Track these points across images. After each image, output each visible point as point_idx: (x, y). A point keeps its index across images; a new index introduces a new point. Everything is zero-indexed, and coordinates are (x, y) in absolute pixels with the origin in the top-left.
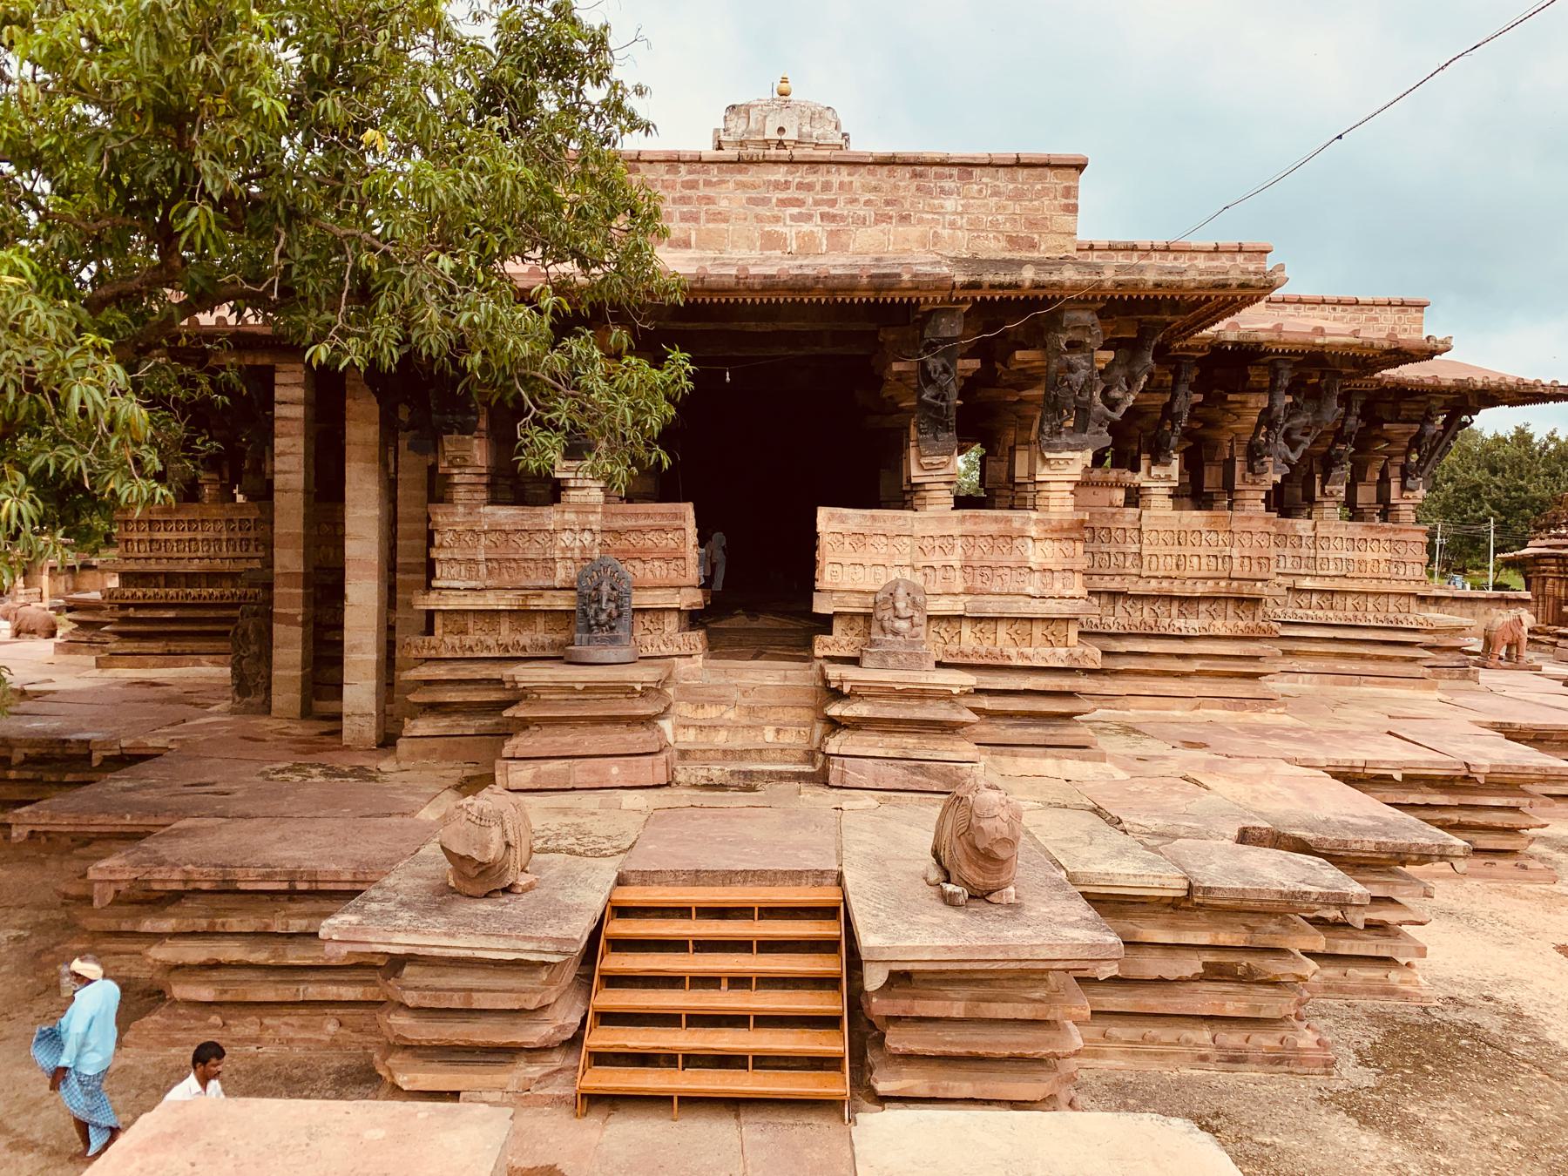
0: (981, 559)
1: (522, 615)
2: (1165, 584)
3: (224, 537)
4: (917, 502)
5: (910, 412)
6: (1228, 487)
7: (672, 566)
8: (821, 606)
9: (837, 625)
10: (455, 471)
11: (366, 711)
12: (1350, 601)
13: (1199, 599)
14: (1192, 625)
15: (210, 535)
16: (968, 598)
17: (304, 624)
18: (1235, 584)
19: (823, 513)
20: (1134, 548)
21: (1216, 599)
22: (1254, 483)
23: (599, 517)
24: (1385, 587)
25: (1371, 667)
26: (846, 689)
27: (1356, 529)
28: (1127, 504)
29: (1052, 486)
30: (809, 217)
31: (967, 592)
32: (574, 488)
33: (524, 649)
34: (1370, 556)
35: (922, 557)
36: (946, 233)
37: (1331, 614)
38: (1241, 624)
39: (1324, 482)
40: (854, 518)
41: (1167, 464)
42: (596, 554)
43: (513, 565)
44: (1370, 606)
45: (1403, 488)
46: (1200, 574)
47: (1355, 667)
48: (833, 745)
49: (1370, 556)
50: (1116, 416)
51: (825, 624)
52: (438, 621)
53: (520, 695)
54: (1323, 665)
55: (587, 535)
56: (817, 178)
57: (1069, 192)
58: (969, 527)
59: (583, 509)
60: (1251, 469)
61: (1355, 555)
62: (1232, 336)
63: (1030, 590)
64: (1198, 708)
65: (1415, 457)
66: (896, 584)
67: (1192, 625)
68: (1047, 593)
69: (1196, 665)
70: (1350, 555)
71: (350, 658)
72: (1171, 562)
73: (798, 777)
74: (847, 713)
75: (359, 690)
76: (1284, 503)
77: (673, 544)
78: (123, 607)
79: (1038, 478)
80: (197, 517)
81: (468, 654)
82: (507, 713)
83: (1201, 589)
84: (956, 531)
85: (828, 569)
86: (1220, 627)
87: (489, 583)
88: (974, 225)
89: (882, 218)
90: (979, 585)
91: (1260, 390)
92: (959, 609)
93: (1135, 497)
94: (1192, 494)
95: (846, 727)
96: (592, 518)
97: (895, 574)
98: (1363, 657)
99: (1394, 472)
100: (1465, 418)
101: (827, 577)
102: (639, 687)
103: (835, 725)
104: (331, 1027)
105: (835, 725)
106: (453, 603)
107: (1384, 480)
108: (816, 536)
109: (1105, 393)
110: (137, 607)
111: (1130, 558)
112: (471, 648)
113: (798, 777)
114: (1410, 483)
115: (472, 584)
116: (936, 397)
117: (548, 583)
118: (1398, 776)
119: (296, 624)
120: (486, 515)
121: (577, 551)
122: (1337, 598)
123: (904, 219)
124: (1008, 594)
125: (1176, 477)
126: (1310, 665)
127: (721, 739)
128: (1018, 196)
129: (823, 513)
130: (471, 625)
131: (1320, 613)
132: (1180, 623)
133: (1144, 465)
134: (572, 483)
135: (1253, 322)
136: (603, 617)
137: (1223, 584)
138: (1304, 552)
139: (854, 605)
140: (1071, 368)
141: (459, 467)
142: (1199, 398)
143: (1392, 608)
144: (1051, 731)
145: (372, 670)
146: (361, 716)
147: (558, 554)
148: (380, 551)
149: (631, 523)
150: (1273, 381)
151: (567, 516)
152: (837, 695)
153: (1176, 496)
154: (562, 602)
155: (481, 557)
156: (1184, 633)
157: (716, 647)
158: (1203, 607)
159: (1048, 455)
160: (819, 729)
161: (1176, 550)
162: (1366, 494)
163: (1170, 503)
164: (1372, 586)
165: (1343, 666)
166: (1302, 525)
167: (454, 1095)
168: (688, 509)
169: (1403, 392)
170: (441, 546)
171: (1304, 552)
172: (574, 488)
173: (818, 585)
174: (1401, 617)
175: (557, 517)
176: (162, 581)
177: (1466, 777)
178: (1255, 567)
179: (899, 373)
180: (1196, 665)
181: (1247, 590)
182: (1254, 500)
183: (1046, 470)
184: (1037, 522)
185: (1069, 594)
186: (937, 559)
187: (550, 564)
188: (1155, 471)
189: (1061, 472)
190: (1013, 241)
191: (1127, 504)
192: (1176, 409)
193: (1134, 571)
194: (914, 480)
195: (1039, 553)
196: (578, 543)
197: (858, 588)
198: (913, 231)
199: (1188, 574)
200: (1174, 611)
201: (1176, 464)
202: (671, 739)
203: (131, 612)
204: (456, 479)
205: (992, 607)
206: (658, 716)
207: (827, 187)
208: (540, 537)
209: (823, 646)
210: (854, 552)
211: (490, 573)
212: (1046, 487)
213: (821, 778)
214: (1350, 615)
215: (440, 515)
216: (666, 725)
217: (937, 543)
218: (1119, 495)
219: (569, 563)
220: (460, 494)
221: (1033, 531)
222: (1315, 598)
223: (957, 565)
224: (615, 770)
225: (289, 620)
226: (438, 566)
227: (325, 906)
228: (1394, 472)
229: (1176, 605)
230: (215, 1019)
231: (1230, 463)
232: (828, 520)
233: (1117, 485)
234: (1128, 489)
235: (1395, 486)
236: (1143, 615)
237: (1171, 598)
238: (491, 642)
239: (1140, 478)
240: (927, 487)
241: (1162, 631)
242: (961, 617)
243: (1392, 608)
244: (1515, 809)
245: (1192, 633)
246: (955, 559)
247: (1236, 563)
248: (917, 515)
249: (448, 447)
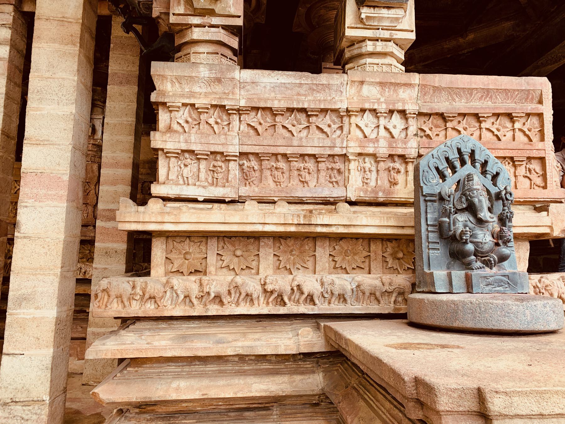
1: (298, 242)
7: (521, 171)
10: (196, 20)
11: (34, 395)
23: (414, 92)
32: (372, 54)
33: (311, 299)
43: (282, 164)
52: (158, 251)
55: (396, 119)
81: (214, 310)
87: (244, 191)
106: (189, 219)
112: (218, 299)
117: (337, 192)
120: (242, 85)
121: (383, 143)
130: (212, 259)
134: (369, 47)
136: (485, 238)
145: (47, 333)
146: (25, 403)
148: (74, 166)
149: (461, 105)
151: (366, 90)
154: (370, 222)
170: (169, 129)
172: (372, 54)
175: (351, 91)
187: (339, 165)
196: (382, 132)
204: (196, 34)
208: (324, 121)
211: (246, 178)
215: (168, 78)
219: (369, 163)
226: (162, 164)
238: (252, 285)
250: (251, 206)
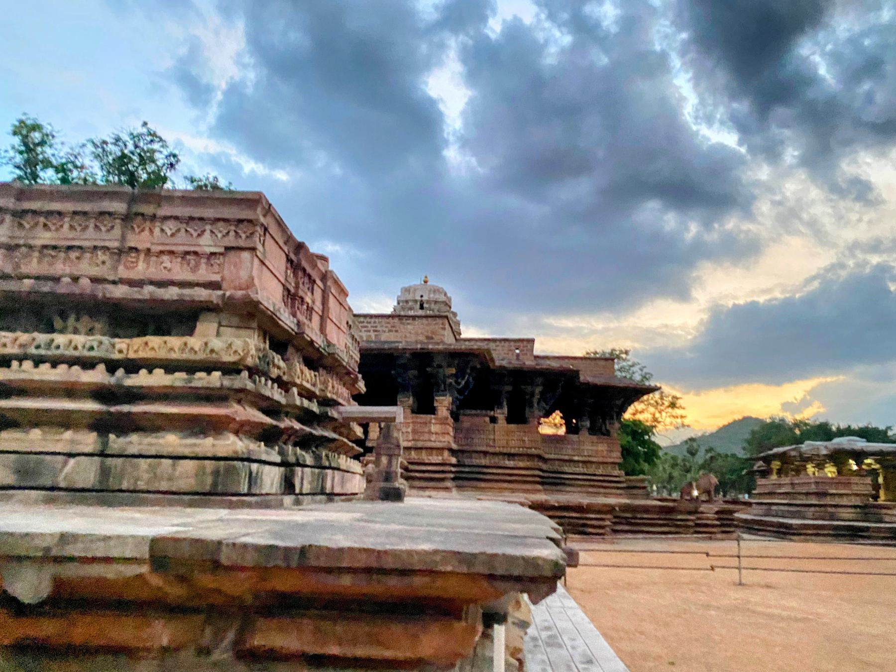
14: (511, 463)
20: (492, 437)
24: (605, 460)
30: (369, 331)
31: (413, 440)
36: (408, 335)
50: (460, 387)
56: (373, 320)
61: (594, 448)
67: (511, 463)
86: (521, 464)
88: (417, 334)
89: (390, 331)
92: (410, 444)
93: (494, 420)
123: (396, 331)
128: (428, 325)
132: (507, 462)
153: (509, 420)
161: (506, 438)
164: (601, 460)
165: (590, 490)
189: (444, 403)
190: (427, 337)
198: (399, 335)
205: (420, 444)
207: (375, 322)
218: (487, 419)
233: (487, 415)
236: (496, 460)
237: (505, 454)
246: (410, 430)
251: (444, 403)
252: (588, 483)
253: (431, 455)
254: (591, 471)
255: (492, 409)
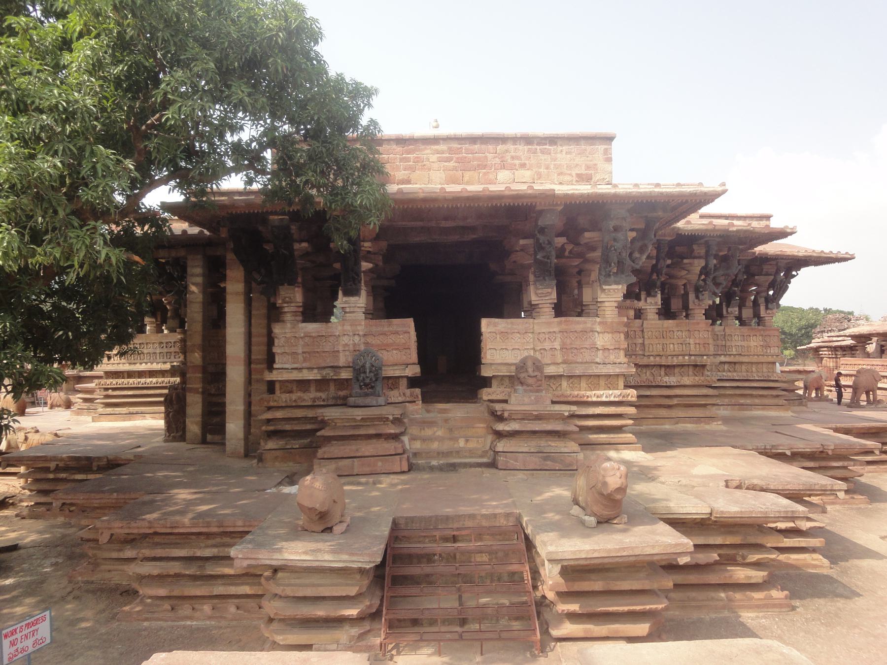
0: (571, 344)
1: (322, 384)
2: (658, 359)
3: (158, 351)
4: (534, 314)
5: (529, 266)
6: (686, 307)
7: (403, 353)
8: (486, 372)
9: (494, 383)
12: (744, 367)
13: (674, 366)
14: (671, 380)
15: (151, 351)
16: (564, 366)
17: (203, 393)
18: (693, 357)
19: (484, 322)
20: (640, 341)
21: (683, 366)
22: (699, 305)
24: (762, 359)
25: (757, 401)
26: (506, 415)
27: (745, 329)
28: (636, 318)
29: (607, 304)
31: (564, 362)
34: (752, 344)
35: (539, 344)
37: (735, 374)
38: (696, 378)
39: (728, 306)
40: (501, 324)
41: (655, 296)
42: (362, 348)
44: (754, 369)
45: (767, 308)
46: (674, 353)
47: (748, 401)
48: (501, 446)
49: (752, 344)
51: (486, 382)
52: (277, 386)
53: (323, 424)
54: (733, 401)
57: (606, 152)
58: (564, 327)
59: (354, 324)
60: (697, 297)
61: (743, 343)
62: (689, 227)
63: (598, 360)
64: (677, 423)
65: (771, 293)
66: (526, 358)
67: (671, 380)
68: (607, 361)
69: (675, 401)
70: (743, 343)
71: (229, 408)
72: (660, 347)
73: (480, 465)
74: (507, 428)
75: (234, 427)
76: (714, 314)
77: (403, 341)
78: (106, 389)
79: (599, 300)
80: (144, 341)
82: (319, 434)
83: (675, 361)
84: (556, 329)
85: (489, 352)
86: (687, 381)
87: (304, 365)
90: (570, 358)
91: (700, 257)
94: (666, 313)
95: (506, 436)
96: (359, 328)
97: (526, 354)
98: (751, 396)
99: (762, 301)
100: (794, 273)
101: (488, 357)
102: (391, 418)
103: (499, 435)
104: (233, 609)
105: (499, 435)
106: (285, 376)
107: (756, 303)
108: (480, 334)
109: (631, 255)
110: (114, 389)
111: (638, 346)
112: (295, 401)
113: (480, 465)
114: (770, 306)
115: (295, 366)
116: (544, 257)
118: (788, 453)
119: (198, 393)
122: (737, 366)
123: (523, 166)
124: (586, 362)
125: (660, 303)
126: (726, 401)
127: (435, 445)
129: (484, 322)
131: (729, 374)
132: (666, 379)
133: (643, 296)
135: (693, 222)
137: (687, 358)
138: (719, 343)
139: (504, 371)
140: (615, 240)
141: (287, 303)
142: (669, 262)
143: (765, 370)
144: (612, 436)
147: (341, 348)
150: (707, 252)
152: (500, 419)
155: (300, 351)
156: (668, 384)
157: (427, 399)
158: (677, 370)
159: (605, 287)
160: (490, 438)
161: (662, 341)
162: (747, 313)
163: (657, 316)
164: (755, 359)
165: (742, 401)
166: (717, 328)
167: (308, 647)
168: (410, 323)
169: (765, 259)
171: (719, 343)
173: (483, 361)
174: (770, 374)
176: (126, 375)
177: (822, 452)
178: (702, 349)
179: (523, 245)
180: (675, 401)
181: (699, 361)
182: (699, 314)
183: (603, 295)
184: (600, 323)
185: (618, 363)
186: (547, 345)
188: (649, 300)
191: (636, 318)
192: (659, 266)
193: (641, 353)
194: (533, 303)
195: (602, 340)
197: (505, 362)
199: (668, 353)
200: (663, 373)
201: (659, 296)
202: (408, 447)
203: (110, 392)
204: (286, 310)
206: (402, 434)
209: (486, 394)
210: (503, 343)
211: (305, 360)
212: (603, 305)
213: (493, 465)
214: (745, 374)
215: (277, 329)
216: (405, 439)
217: (547, 336)
218: (632, 313)
219: (347, 353)
220: (288, 317)
221: (598, 328)
222: (726, 367)
223: (558, 347)
224: (380, 464)
225: (195, 391)
227: (227, 540)
228: (762, 301)
229: (663, 369)
230: (167, 606)
231: (685, 297)
232: (487, 326)
234: (635, 310)
235: (762, 308)
237: (661, 366)
239: (641, 304)
240: (540, 306)
241: (657, 384)
242: (561, 376)
243: (765, 370)
244: (845, 468)
245: (672, 384)
246: (557, 345)
247: (692, 346)
248: (536, 321)
249: (282, 293)
250: (305, 371)
251: (610, 295)
252: (738, 392)
253: (597, 387)
254: (743, 375)
255: (639, 299)
